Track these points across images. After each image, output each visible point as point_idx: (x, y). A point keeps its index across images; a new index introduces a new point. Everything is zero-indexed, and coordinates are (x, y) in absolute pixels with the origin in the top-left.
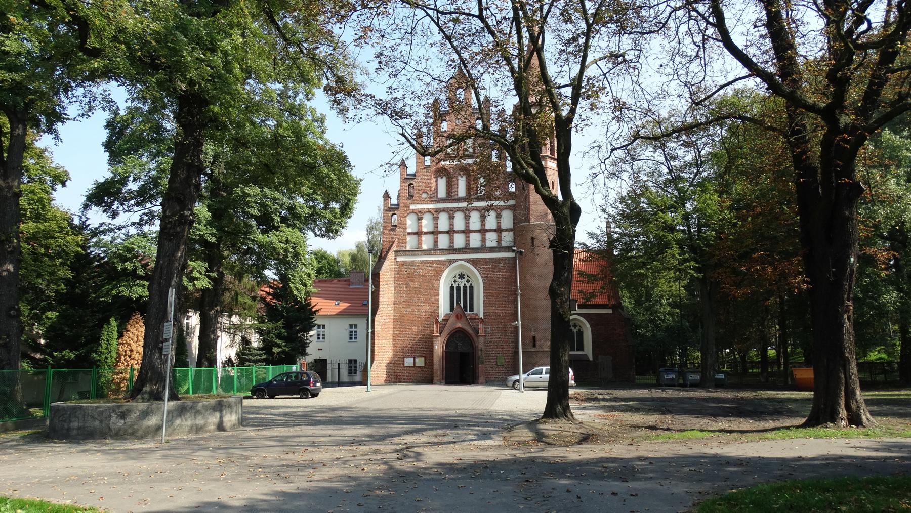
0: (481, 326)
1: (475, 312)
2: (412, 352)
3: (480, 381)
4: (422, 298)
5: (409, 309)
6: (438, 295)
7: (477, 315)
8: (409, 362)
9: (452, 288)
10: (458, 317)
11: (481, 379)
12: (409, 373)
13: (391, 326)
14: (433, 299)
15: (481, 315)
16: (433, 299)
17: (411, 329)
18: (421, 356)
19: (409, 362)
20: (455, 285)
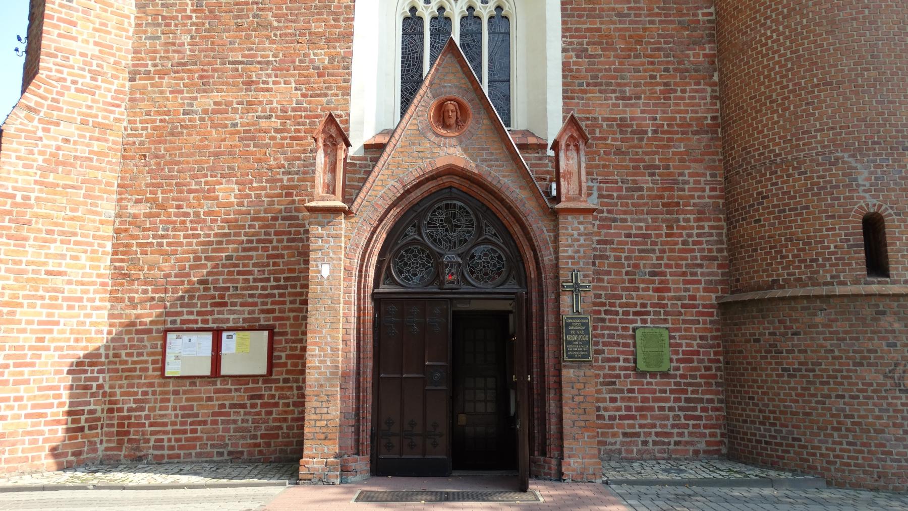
0: (568, 162)
1: (520, 120)
2: (206, 307)
3: (572, 464)
4: (269, 51)
5: (205, 102)
6: (348, 36)
7: (527, 133)
8: (188, 354)
9: (412, 23)
10: (445, 117)
11: (578, 455)
12: (187, 413)
13: (111, 176)
14: (320, 56)
15: (553, 127)
16: (320, 56)
17: (209, 194)
18: (251, 327)
19: (188, 354)
20: (427, 13)
